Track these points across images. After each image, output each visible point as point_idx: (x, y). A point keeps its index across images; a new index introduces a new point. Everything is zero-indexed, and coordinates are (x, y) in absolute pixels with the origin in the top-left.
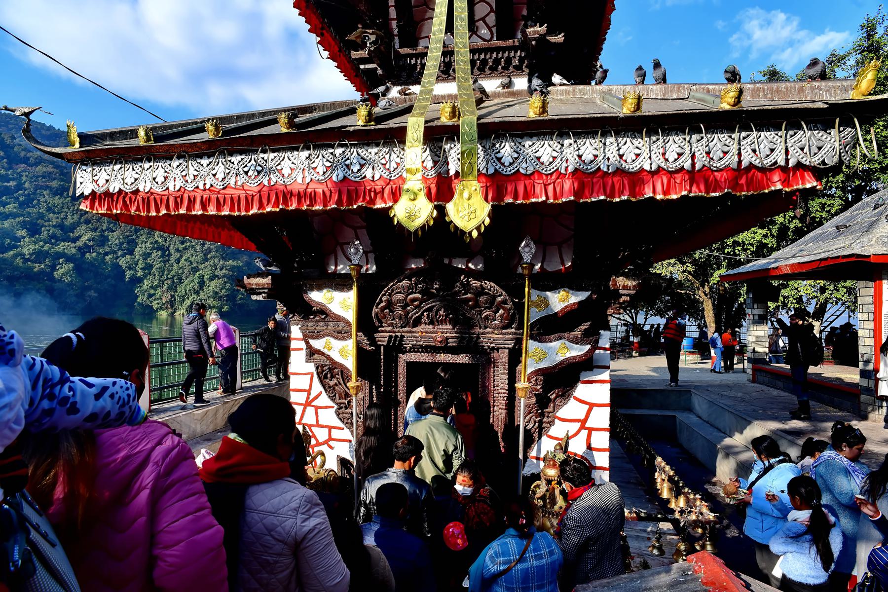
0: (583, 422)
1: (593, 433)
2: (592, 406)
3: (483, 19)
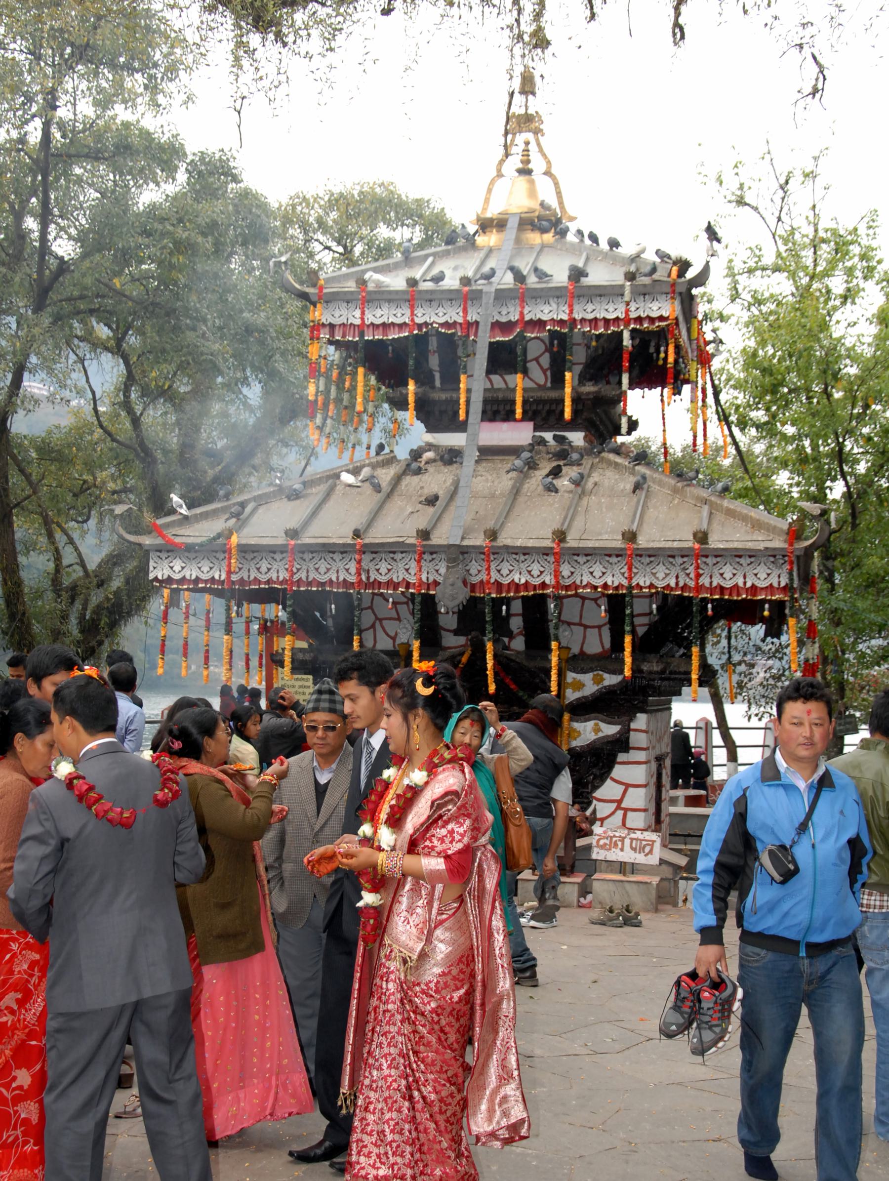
0: (620, 802)
1: (630, 814)
2: (627, 786)
3: (536, 359)
